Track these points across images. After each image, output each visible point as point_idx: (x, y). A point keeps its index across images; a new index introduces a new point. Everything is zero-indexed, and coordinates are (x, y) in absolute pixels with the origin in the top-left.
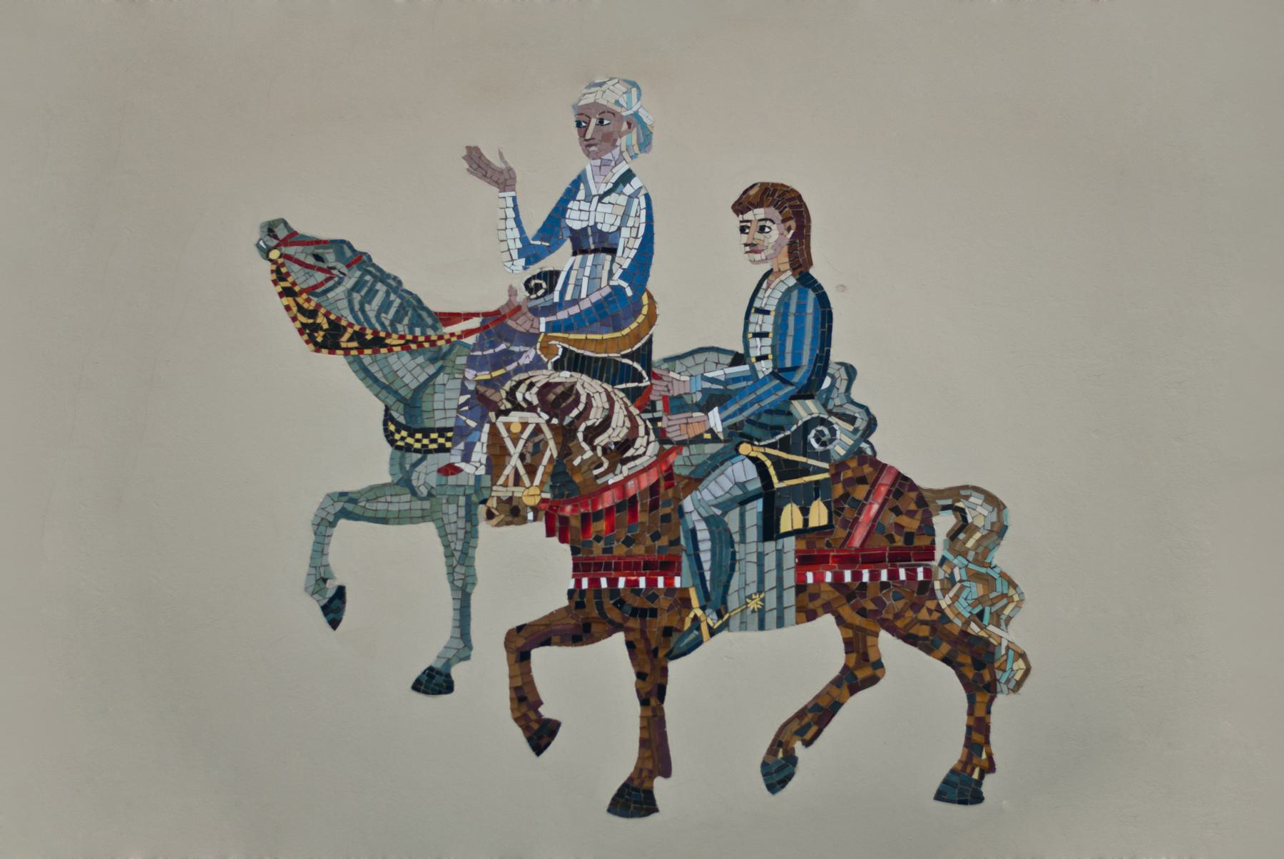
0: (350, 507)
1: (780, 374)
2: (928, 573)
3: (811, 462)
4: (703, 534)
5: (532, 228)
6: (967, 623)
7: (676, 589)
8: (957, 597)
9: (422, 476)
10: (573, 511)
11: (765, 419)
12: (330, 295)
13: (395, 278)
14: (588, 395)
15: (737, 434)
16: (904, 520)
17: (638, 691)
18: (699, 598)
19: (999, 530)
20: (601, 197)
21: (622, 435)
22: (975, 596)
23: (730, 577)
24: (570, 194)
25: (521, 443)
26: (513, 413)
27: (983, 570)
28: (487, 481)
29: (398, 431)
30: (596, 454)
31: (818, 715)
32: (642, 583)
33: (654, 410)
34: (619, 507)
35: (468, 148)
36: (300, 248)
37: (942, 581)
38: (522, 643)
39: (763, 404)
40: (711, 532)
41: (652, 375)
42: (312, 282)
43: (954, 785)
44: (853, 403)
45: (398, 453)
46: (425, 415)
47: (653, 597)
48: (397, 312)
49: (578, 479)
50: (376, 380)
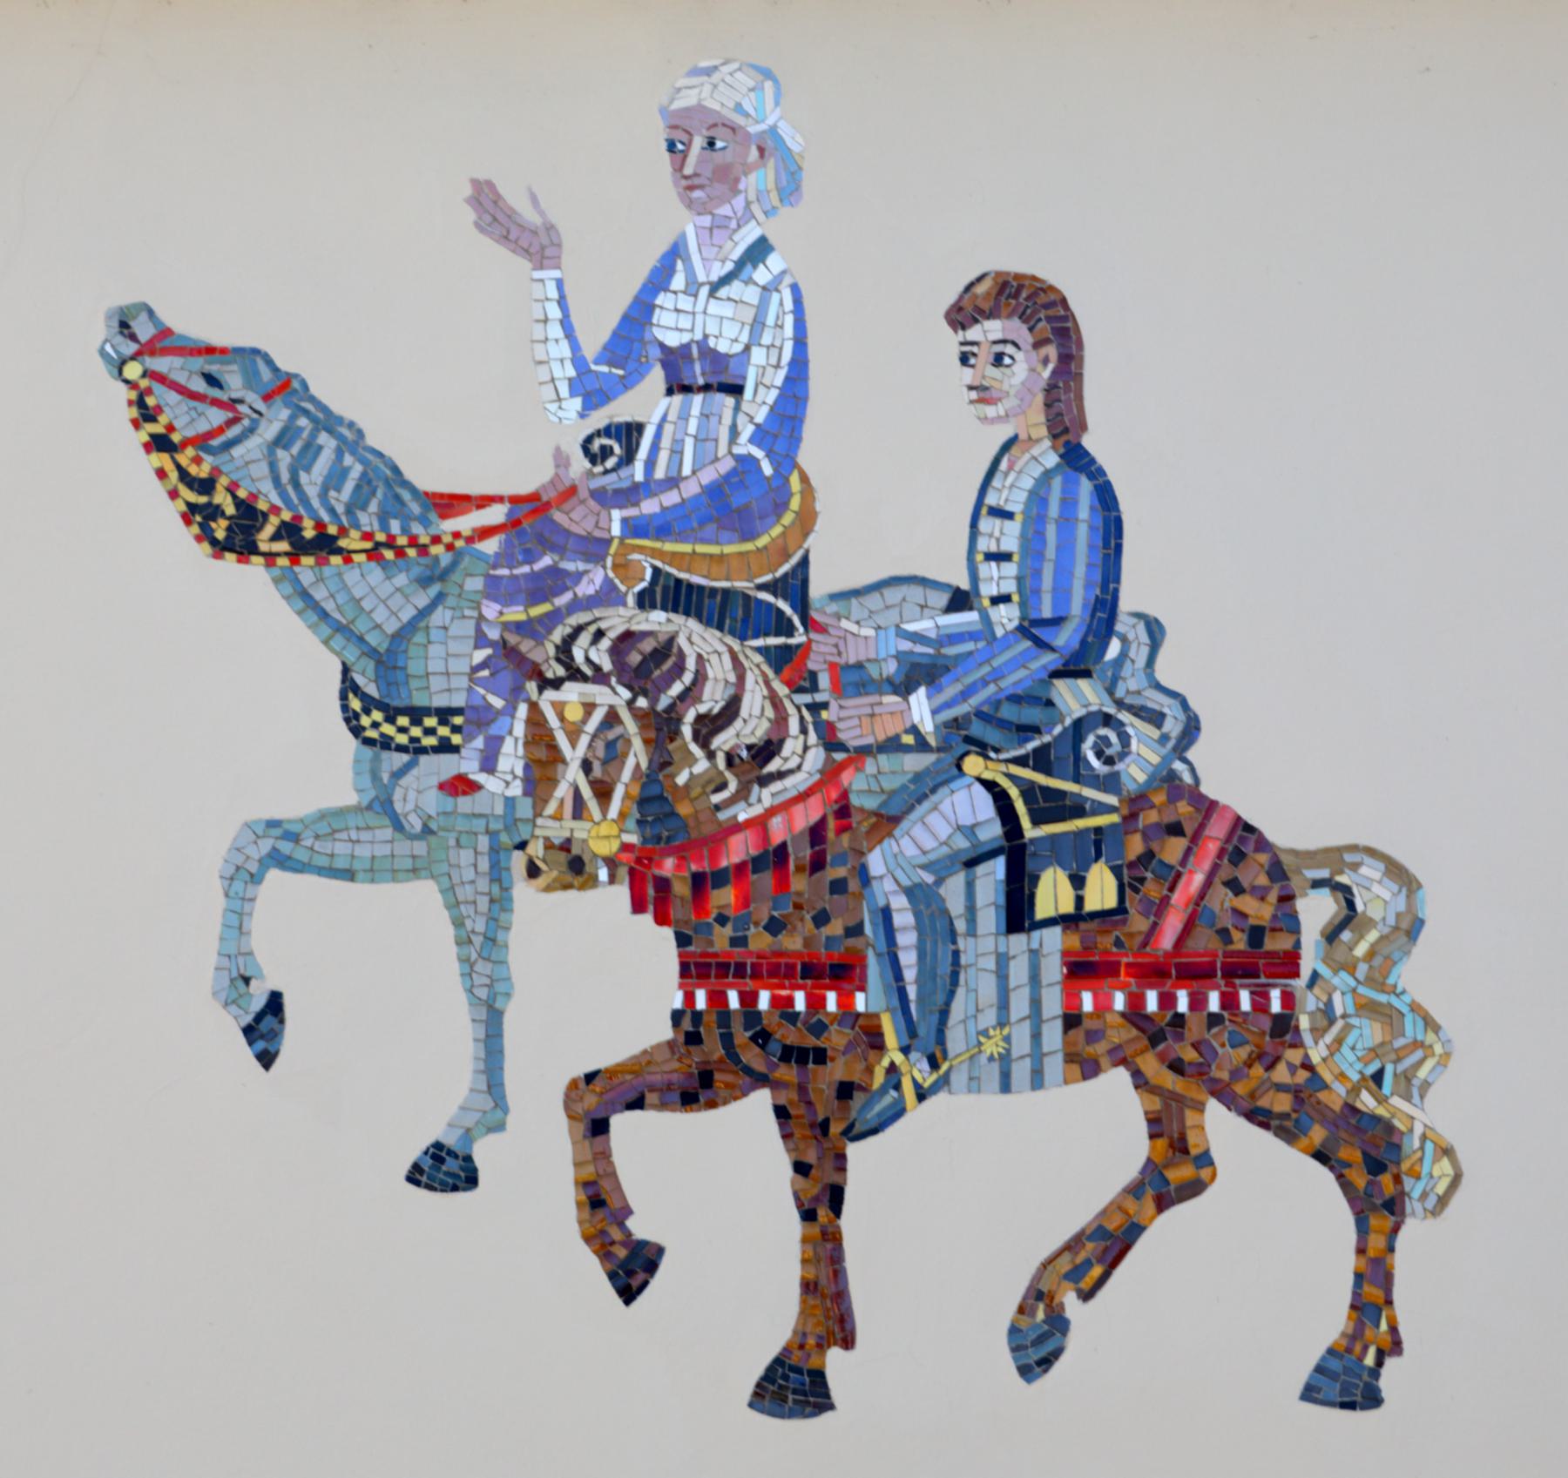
0: (286, 847)
1: (1032, 630)
2: (1288, 999)
3: (1089, 793)
4: (903, 918)
5: (594, 340)
6: (1355, 1090)
7: (858, 1015)
8: (1339, 1041)
9: (412, 795)
10: (678, 867)
11: (1008, 712)
12: (237, 451)
13: (351, 425)
14: (700, 657)
15: (962, 738)
16: (1248, 904)
17: (796, 1195)
18: (897, 1031)
19: (1411, 928)
20: (715, 288)
21: (760, 733)
22: (1369, 1044)
23: (952, 994)
24: (659, 280)
25: (584, 741)
26: (568, 685)
27: (1383, 998)
28: (525, 808)
29: (367, 712)
30: (715, 766)
31: (1105, 1247)
32: (800, 1002)
33: (814, 688)
34: (757, 864)
35: (476, 184)
36: (177, 361)
37: (1311, 1014)
38: (598, 1103)
39: (1004, 684)
40: (917, 914)
41: (808, 622)
42: (203, 427)
43: (1333, 1376)
44: (1159, 687)
45: (368, 752)
46: (414, 684)
47: (819, 1029)
48: (358, 487)
49: (684, 809)
50: (324, 615)
